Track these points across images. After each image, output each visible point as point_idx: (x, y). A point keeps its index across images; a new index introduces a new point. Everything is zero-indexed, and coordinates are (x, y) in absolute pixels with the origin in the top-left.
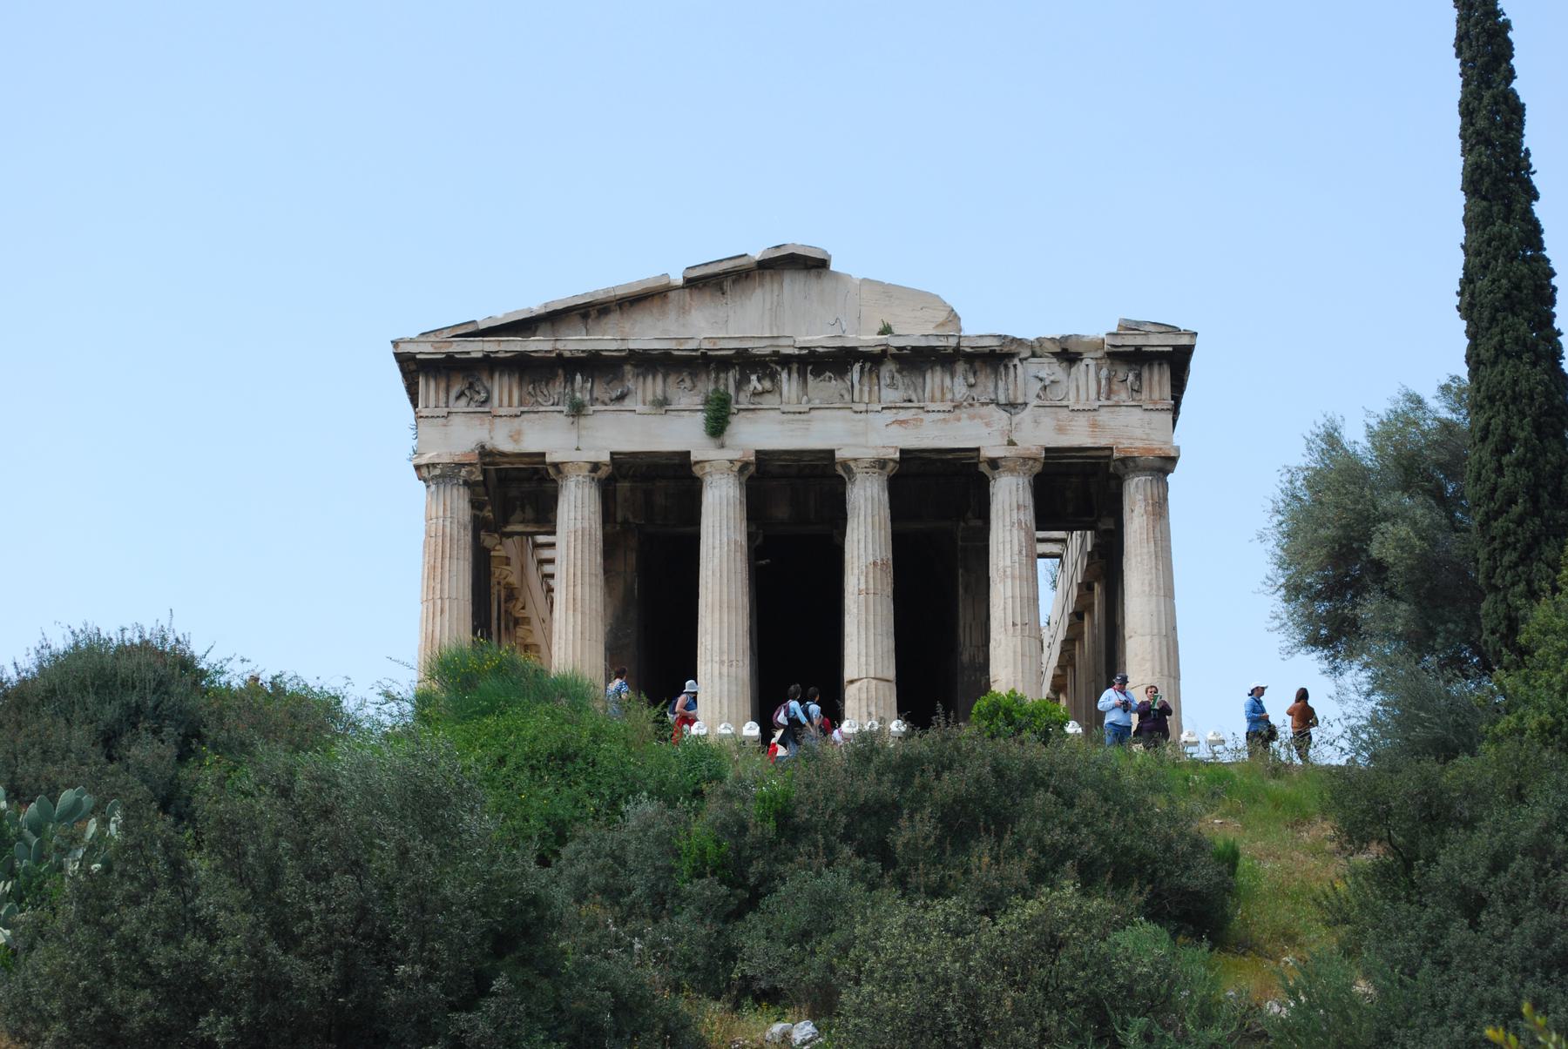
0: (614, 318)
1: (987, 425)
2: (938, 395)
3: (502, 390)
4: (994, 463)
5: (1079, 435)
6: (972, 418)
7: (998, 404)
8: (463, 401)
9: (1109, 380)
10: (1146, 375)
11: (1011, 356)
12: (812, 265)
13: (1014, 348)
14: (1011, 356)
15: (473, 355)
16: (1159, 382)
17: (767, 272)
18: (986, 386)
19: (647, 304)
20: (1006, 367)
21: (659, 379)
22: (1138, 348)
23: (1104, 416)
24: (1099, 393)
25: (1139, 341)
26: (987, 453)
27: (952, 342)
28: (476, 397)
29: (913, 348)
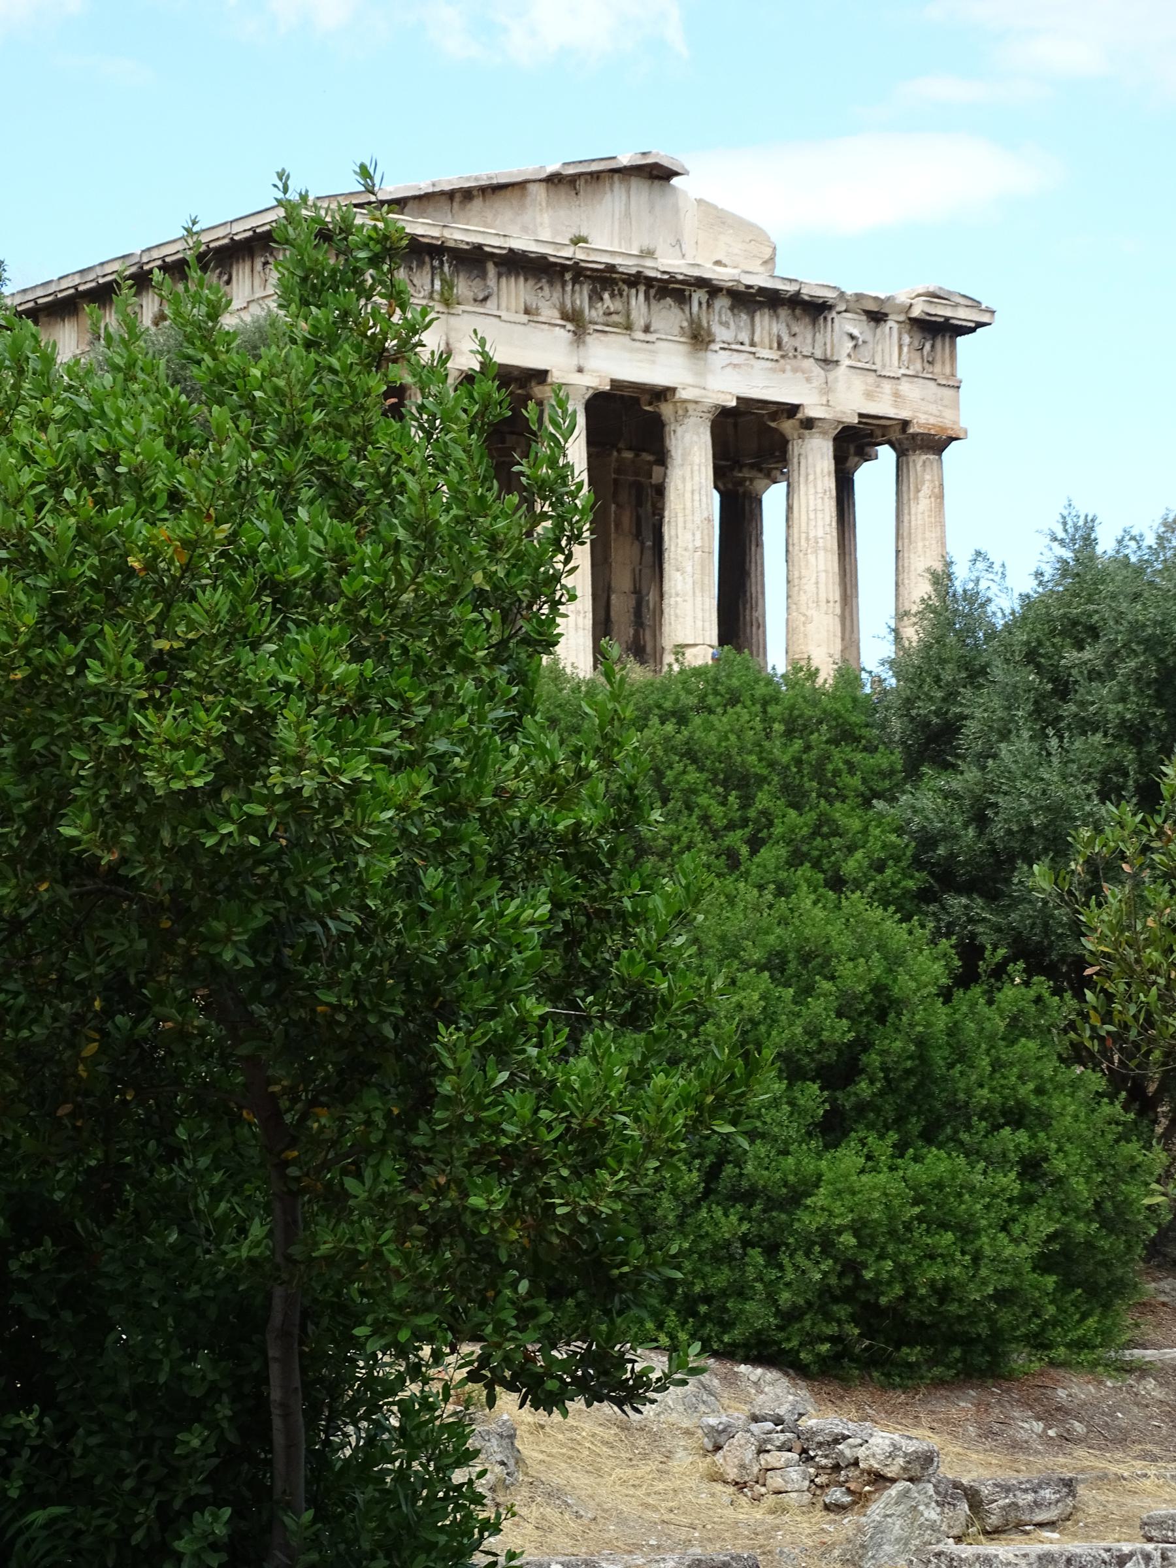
0: (477, 203)
1: (808, 380)
2: (767, 341)
4: (809, 424)
5: (883, 407)
6: (795, 370)
11: (830, 308)
14: (830, 308)
17: (616, 176)
18: (804, 337)
21: (522, 279)
22: (947, 319)
23: (905, 386)
25: (948, 313)
26: (812, 412)
27: (792, 288)
29: (762, 290)
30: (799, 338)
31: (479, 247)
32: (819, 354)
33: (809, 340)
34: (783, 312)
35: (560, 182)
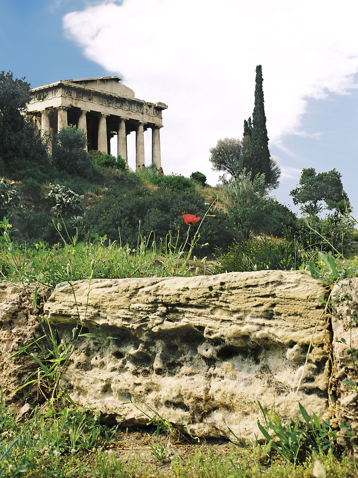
0: (89, 84)
3: (74, 95)
4: (140, 123)
23: (154, 118)
31: (90, 90)
35: (103, 81)
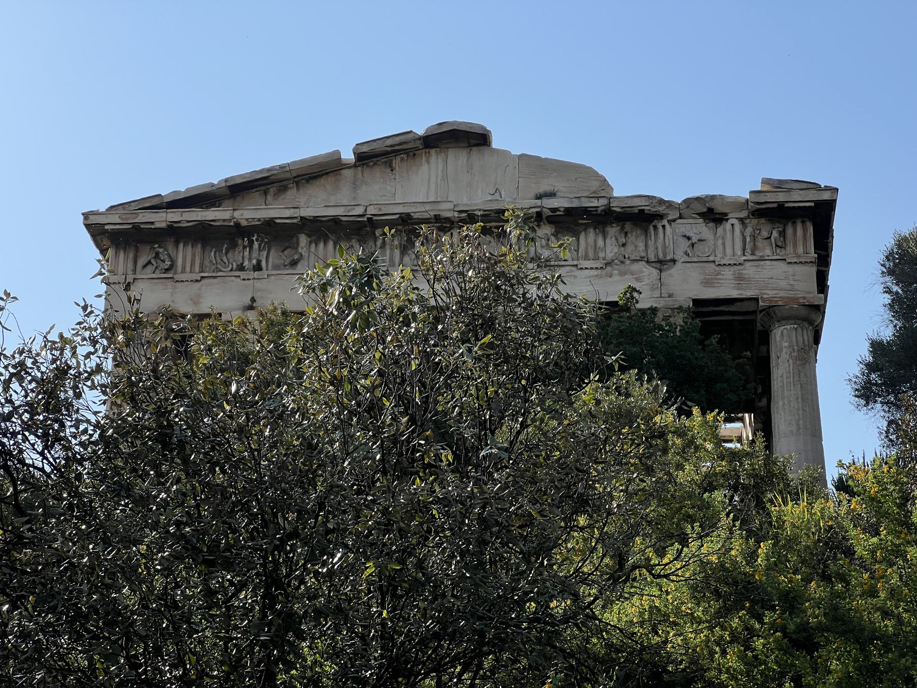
5: (726, 290)
7: (648, 262)
8: (150, 269)
9: (754, 238)
10: (789, 231)
11: (661, 217)
12: (473, 139)
13: (661, 209)
14: (661, 217)
15: (157, 225)
16: (802, 237)
18: (637, 244)
19: (322, 181)
20: (655, 227)
22: (781, 205)
23: (749, 270)
24: (744, 250)
25: (781, 197)
28: (161, 264)
29: (568, 211)
30: (630, 248)
32: (652, 258)
33: (641, 246)
34: (613, 230)
